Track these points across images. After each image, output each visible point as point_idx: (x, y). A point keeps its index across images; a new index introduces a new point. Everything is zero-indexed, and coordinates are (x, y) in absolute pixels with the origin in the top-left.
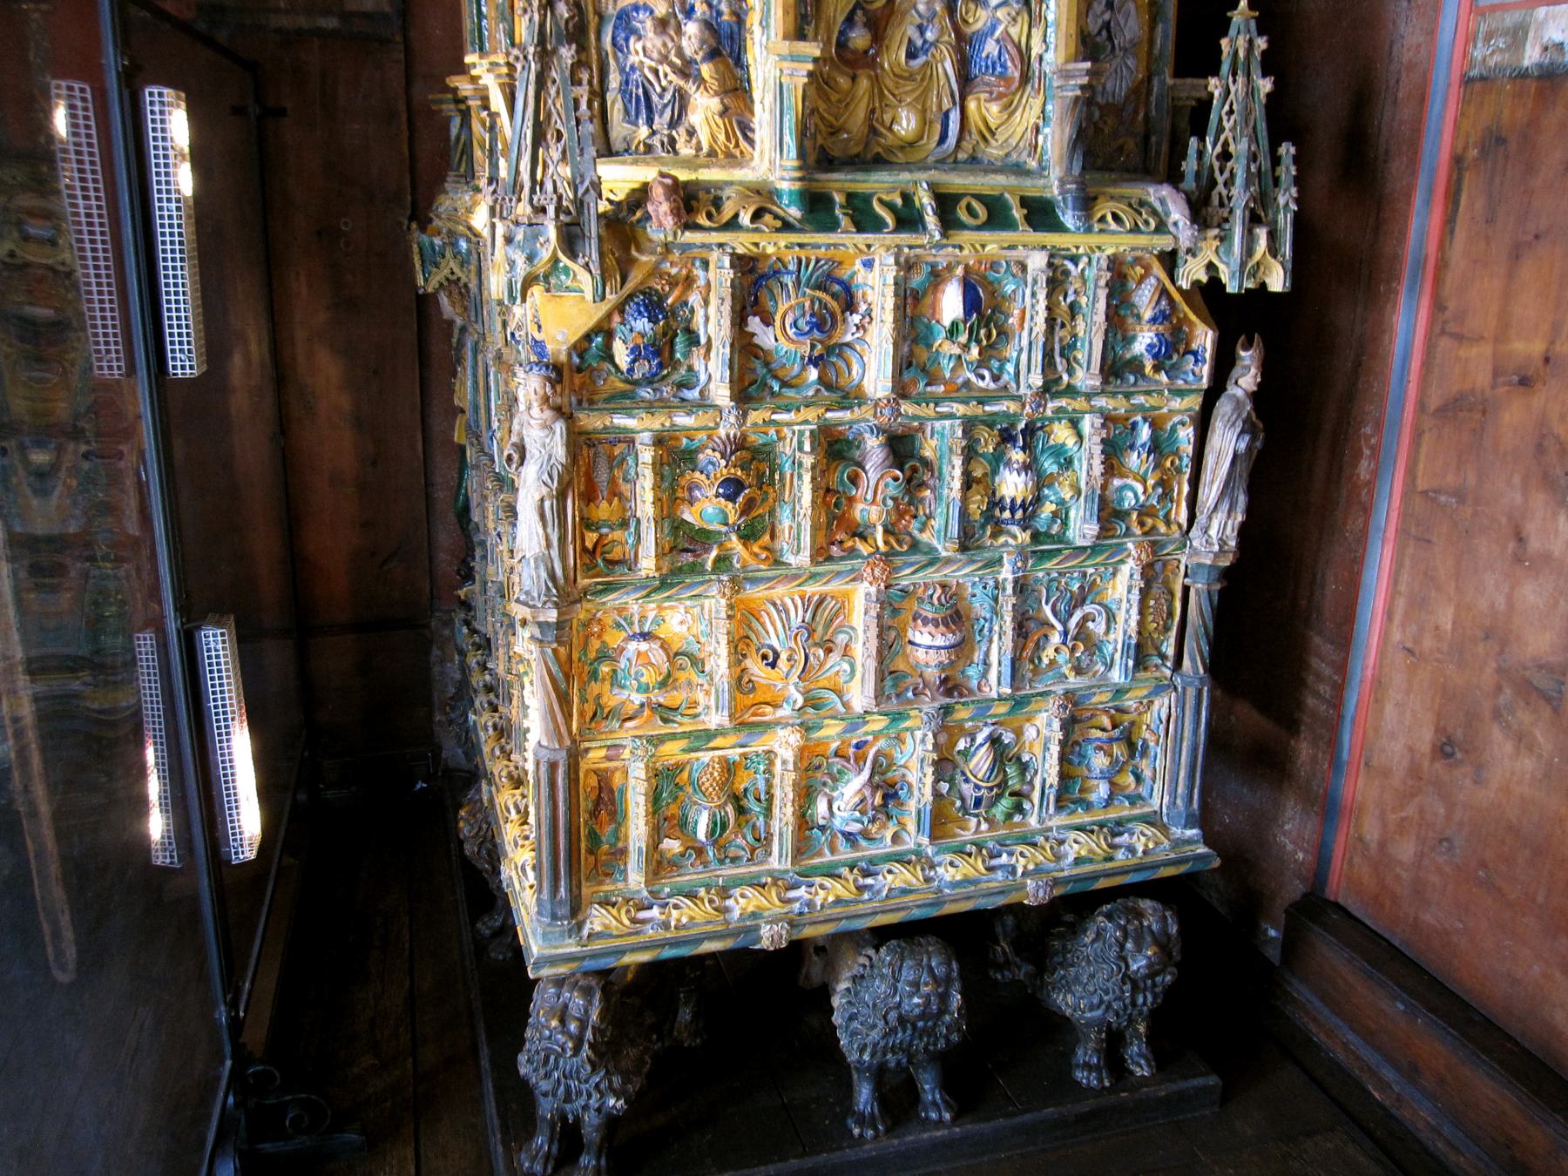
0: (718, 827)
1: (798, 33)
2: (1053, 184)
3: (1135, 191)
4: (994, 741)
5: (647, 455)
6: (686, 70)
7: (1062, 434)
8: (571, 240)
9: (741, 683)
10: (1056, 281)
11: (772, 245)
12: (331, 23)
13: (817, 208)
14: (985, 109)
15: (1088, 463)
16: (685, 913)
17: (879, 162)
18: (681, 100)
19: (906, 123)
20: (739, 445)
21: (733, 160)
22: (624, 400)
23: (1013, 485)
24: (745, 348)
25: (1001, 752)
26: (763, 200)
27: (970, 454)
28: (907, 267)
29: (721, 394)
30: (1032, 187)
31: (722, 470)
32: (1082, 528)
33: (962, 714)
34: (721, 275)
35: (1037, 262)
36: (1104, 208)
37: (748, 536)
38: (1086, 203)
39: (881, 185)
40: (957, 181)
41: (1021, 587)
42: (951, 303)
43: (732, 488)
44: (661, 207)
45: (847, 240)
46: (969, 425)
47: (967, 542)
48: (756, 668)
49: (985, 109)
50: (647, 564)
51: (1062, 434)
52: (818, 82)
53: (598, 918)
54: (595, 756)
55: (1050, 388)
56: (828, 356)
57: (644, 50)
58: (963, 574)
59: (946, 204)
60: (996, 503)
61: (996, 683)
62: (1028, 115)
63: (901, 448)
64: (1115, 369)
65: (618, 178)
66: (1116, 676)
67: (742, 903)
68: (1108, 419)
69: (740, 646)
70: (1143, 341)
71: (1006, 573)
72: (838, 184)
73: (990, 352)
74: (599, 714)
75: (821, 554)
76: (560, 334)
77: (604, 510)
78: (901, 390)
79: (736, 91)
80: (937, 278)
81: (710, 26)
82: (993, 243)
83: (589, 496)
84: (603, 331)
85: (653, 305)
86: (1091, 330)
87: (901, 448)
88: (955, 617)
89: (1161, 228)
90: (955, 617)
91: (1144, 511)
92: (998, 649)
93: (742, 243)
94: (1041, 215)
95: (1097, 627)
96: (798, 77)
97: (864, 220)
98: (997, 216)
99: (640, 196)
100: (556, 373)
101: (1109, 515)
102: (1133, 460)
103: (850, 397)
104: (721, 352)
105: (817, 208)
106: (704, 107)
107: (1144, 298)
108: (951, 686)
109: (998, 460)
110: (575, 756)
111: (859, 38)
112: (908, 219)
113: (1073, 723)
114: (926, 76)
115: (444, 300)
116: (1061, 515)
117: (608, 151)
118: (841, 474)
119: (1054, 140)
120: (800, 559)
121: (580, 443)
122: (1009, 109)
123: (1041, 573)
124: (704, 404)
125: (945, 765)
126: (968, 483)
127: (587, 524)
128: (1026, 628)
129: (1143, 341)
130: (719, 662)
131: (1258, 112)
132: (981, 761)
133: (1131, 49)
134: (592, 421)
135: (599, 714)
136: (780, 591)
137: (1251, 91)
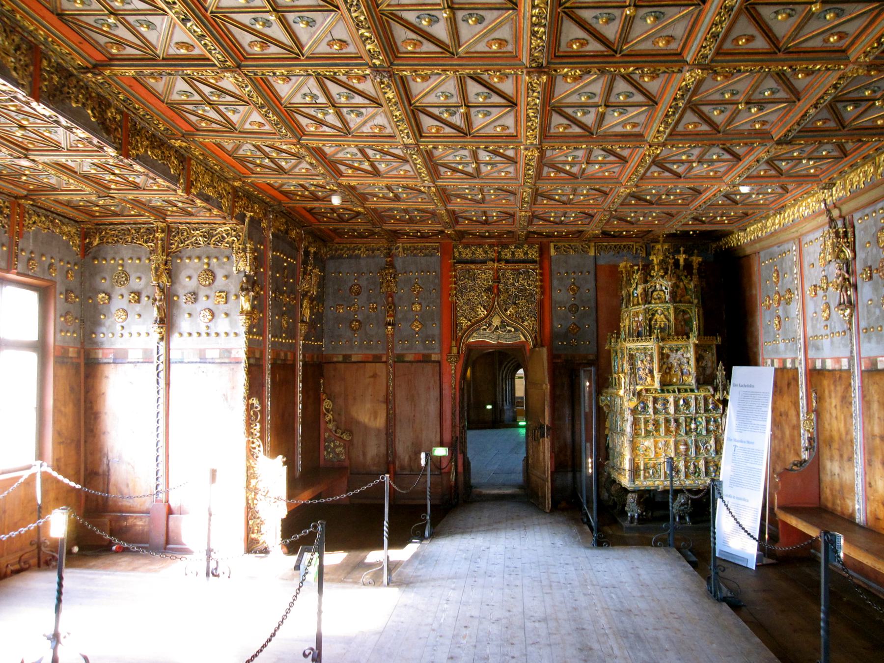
0: (653, 473)
1: (659, 371)
2: (694, 387)
3: (706, 387)
4: (694, 464)
5: (643, 421)
6: (647, 375)
7: (700, 419)
8: (634, 395)
9: (656, 453)
10: (696, 399)
11: (657, 395)
12: (585, 361)
13: (662, 391)
14: (685, 378)
15: (704, 424)
16: (648, 483)
17: (672, 385)
18: (646, 378)
19: (675, 380)
20: (654, 420)
21: (653, 385)
22: (640, 414)
23: (693, 426)
24: (655, 408)
25: (695, 466)
26: (656, 390)
27: (686, 421)
28: (675, 397)
29: (652, 413)
30: (691, 387)
31: (652, 422)
32: (704, 433)
33: (688, 459)
34: (651, 399)
35: (693, 396)
36: (701, 389)
37: (656, 432)
38: (698, 389)
39: (671, 388)
40: (681, 387)
41: (696, 441)
42: (681, 402)
43: (654, 425)
44: (644, 392)
45: (666, 394)
46: (685, 418)
47: (686, 433)
48: (657, 450)
49: (685, 378)
50: (643, 434)
51: (700, 419)
52: (662, 376)
53: (637, 483)
54: (636, 459)
55: (697, 413)
56: (666, 408)
57: (641, 372)
58: (686, 438)
59: (679, 390)
60: (690, 429)
61: (693, 455)
62: (690, 379)
63: (676, 421)
64: (706, 410)
65: (639, 388)
66: (713, 455)
67: (657, 483)
68: (706, 417)
69: (655, 447)
70: (711, 406)
71: (693, 438)
72: (665, 388)
73: (688, 408)
74: (637, 455)
75: (666, 434)
76: (632, 407)
77: (637, 427)
78: (675, 413)
79: (653, 377)
80: (679, 399)
81: (649, 370)
82: (686, 394)
83: (636, 425)
84: (637, 406)
85: (643, 403)
86: (702, 405)
87: (676, 421)
88: (686, 444)
89: (709, 391)
90: (686, 444)
91: (714, 431)
92: (693, 450)
93: (654, 395)
94: (692, 391)
95: (709, 448)
96: (660, 376)
97: (668, 392)
98: (686, 391)
99: (641, 390)
100: (632, 411)
101: (708, 431)
102: (712, 423)
103: (668, 414)
104: (652, 408)
105: (662, 391)
106: (649, 379)
107: (710, 401)
108: (686, 455)
109: (691, 423)
110: (634, 460)
111: (668, 371)
112: (674, 392)
113: (707, 463)
114: (677, 374)
115: (605, 408)
116: (701, 430)
117: (637, 385)
118: (668, 424)
119: (693, 382)
120: (663, 435)
121: (634, 418)
122: (688, 378)
123: (699, 438)
124: (650, 414)
125: (687, 467)
126: (686, 426)
127: (635, 429)
128: (697, 447)
129: (711, 406)
130: (653, 448)
131: (724, 376)
132: (692, 467)
133: (710, 367)
134: (636, 416)
135: (637, 455)
136: (660, 439)
137: (722, 374)
